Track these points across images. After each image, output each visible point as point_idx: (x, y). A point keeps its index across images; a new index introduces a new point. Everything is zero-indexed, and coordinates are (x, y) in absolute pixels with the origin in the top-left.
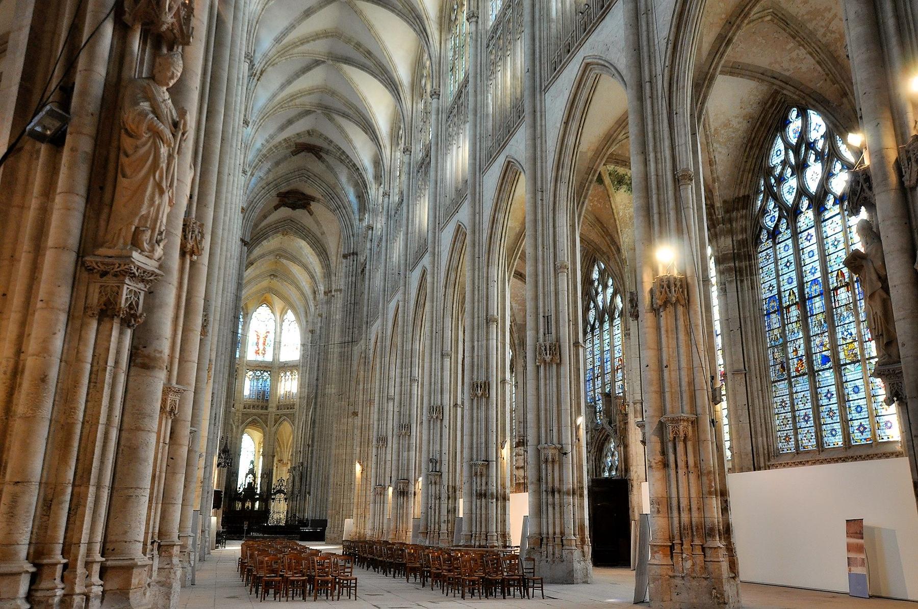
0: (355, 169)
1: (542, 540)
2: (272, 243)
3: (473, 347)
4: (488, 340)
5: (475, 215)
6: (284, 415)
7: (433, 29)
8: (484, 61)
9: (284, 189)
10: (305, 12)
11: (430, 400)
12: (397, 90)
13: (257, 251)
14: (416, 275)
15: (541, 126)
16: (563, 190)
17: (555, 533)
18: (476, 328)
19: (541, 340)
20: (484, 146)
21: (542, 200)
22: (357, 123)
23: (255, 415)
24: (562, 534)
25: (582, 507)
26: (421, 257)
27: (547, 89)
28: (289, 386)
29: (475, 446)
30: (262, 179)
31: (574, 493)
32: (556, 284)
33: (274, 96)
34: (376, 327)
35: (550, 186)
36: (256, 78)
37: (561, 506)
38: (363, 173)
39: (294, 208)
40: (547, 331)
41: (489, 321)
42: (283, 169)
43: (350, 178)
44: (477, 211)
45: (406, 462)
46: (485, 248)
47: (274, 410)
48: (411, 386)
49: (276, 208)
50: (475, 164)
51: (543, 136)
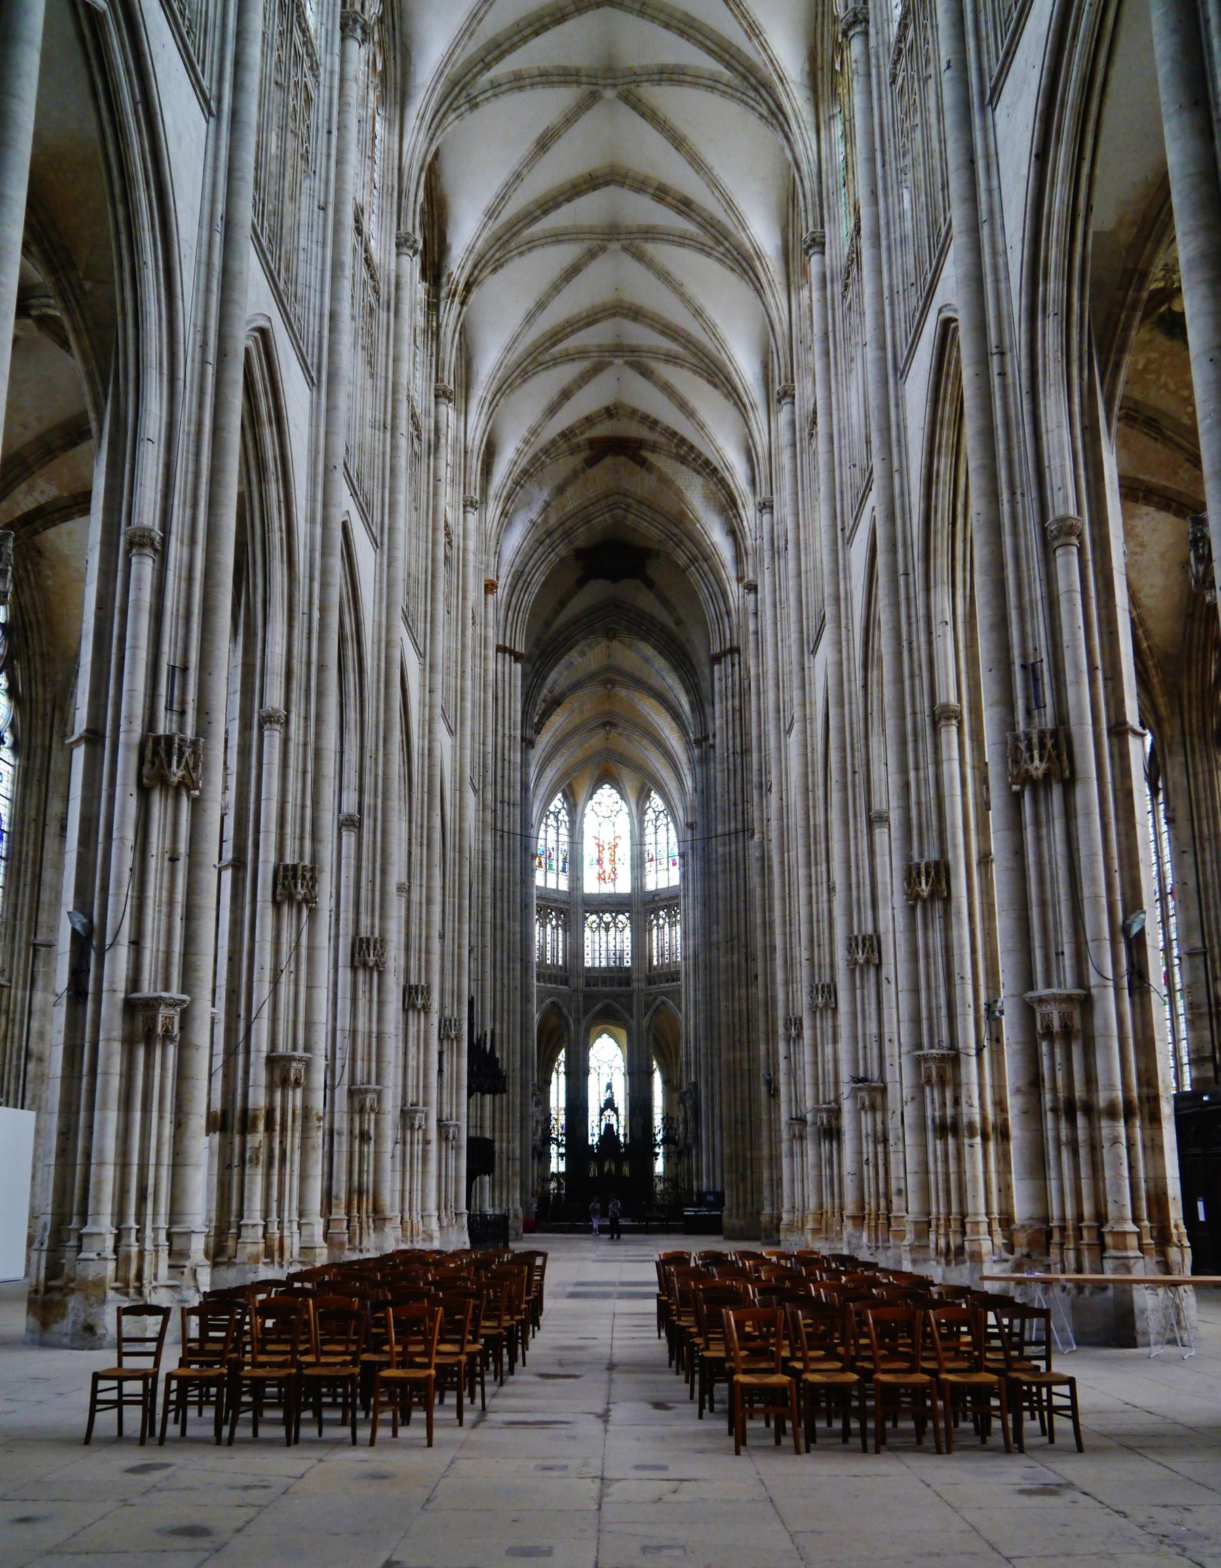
0: (710, 470)
1: (1049, 1234)
2: (585, 658)
3: (906, 785)
4: (938, 763)
5: (891, 478)
6: (662, 994)
7: (796, 99)
8: (887, 119)
9: (582, 537)
12: (753, 269)
13: (558, 677)
17: (1080, 1217)
18: (910, 738)
19: (1021, 727)
20: (900, 312)
21: (1002, 374)
22: (695, 370)
23: (607, 996)
24: (1101, 1217)
25: (1154, 1148)
28: (669, 939)
29: (924, 1014)
30: (533, 523)
31: (1129, 1114)
32: (1050, 579)
36: (457, 300)
37: (1094, 1147)
38: (727, 475)
39: (615, 578)
40: (1034, 703)
41: (940, 716)
42: (573, 500)
43: (710, 498)
44: (896, 465)
47: (643, 985)
49: (581, 583)
50: (885, 359)
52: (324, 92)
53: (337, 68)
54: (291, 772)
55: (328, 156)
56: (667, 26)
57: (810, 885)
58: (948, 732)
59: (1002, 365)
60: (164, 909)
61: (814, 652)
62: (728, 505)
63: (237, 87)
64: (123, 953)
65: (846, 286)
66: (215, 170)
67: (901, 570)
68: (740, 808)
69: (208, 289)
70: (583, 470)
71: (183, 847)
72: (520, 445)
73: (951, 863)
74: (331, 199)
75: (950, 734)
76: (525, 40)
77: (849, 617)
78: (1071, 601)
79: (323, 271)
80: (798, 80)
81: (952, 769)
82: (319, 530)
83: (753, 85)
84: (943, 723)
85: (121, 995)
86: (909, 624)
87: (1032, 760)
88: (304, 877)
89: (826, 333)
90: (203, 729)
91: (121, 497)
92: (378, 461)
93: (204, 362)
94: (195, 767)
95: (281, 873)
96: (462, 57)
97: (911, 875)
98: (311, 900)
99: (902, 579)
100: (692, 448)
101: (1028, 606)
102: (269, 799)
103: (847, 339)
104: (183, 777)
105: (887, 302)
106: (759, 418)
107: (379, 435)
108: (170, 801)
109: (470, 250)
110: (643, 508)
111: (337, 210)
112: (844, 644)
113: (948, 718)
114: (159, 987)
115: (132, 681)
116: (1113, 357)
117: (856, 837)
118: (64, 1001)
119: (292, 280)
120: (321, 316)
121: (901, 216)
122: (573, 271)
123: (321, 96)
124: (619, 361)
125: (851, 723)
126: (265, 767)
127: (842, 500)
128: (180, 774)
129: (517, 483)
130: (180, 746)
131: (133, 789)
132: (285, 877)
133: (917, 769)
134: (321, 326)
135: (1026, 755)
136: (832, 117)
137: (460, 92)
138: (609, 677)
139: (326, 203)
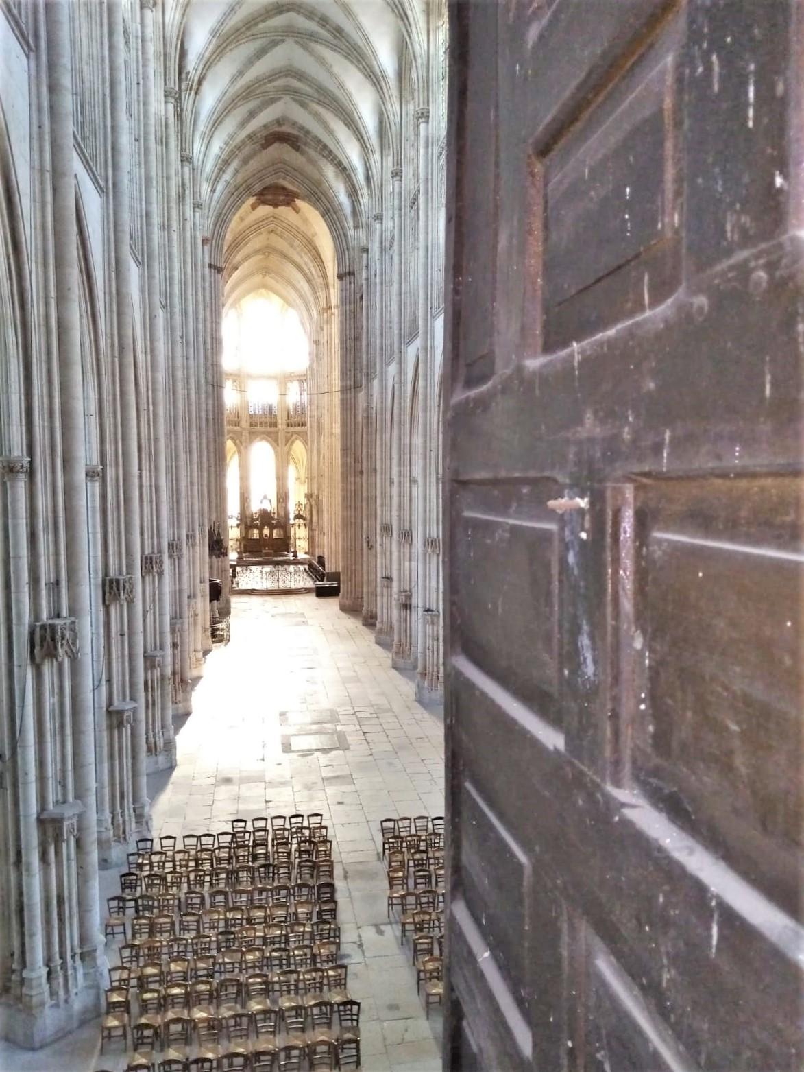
0: (343, 170)
36: (193, 92)
45: (407, 572)
47: (284, 426)
57: (400, 476)
70: (260, 151)
72: (222, 145)
74: (142, 133)
77: (432, 361)
79: (140, 184)
93: (113, 357)
109: (201, 57)
110: (297, 174)
111: (146, 140)
120: (141, 216)
124: (287, 98)
129: (221, 169)
134: (142, 224)
136: (437, 28)
138: (267, 250)
139: (139, 136)
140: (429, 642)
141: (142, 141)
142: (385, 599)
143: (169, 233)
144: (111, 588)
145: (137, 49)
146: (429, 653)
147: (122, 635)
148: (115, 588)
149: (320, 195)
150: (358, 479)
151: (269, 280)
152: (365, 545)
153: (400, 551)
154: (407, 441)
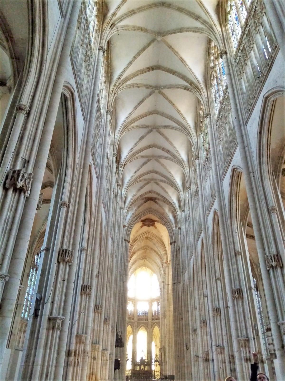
0: (170, 204)
4: (237, 265)
5: (221, 201)
6: (155, 323)
8: (216, 132)
10: (140, 138)
11: (212, 305)
12: (182, 164)
14: (199, 243)
15: (247, 141)
16: (265, 168)
18: (230, 259)
20: (221, 168)
22: (168, 184)
26: (201, 233)
27: (247, 122)
32: (271, 220)
33: (133, 176)
34: (186, 274)
35: (257, 168)
36: (122, 167)
38: (174, 205)
39: (149, 226)
41: (237, 254)
42: (141, 209)
43: (170, 209)
44: (222, 199)
45: (206, 342)
46: (228, 216)
47: (151, 320)
48: (204, 299)
50: (218, 178)
51: (249, 146)
52: (103, 124)
53: (105, 119)
54: (87, 262)
55: (103, 135)
56: (167, 118)
57: (199, 295)
58: (239, 258)
59: (253, 174)
60: (60, 293)
61: (197, 241)
62: (174, 212)
63: (90, 116)
64: (49, 305)
65: (204, 166)
66: (85, 131)
67: (225, 221)
68: (177, 277)
69: (82, 154)
70: (144, 204)
71: (66, 277)
73: (243, 289)
74: (103, 143)
75: (239, 258)
76: (139, 119)
77: (208, 233)
78: (277, 225)
79: (101, 156)
80: (193, 128)
81: (240, 266)
82: (97, 208)
83: (184, 129)
84: (238, 255)
85: (47, 316)
86: (228, 233)
87: (273, 262)
88: (89, 288)
89: (200, 175)
90: (73, 248)
91: (60, 195)
92: (107, 197)
93: (80, 168)
94: (71, 257)
95: (83, 287)
96: (127, 121)
97: (233, 292)
98: (90, 294)
99: (225, 223)
100: (167, 199)
101: (266, 226)
102: (82, 268)
103: (205, 176)
104: (69, 260)
105: (217, 166)
106: (182, 193)
107: (107, 191)
108: (64, 266)
110: (155, 212)
112: (207, 239)
113: (239, 254)
114: (57, 314)
115: (58, 236)
116: (278, 174)
117: (213, 283)
118: (32, 318)
119: (95, 157)
120: (100, 165)
121: (220, 150)
122: (145, 163)
123: (102, 124)
124: (152, 182)
125: (210, 256)
126: (81, 261)
127: (205, 208)
128: (68, 259)
130: (68, 252)
131: (56, 262)
132: (84, 288)
133: (232, 266)
135: (271, 261)
136: (200, 135)
137: (126, 128)
140: (220, 365)
141: (103, 145)
142: (196, 368)
143: (110, 192)
144: (62, 253)
145: (104, 123)
146: (221, 371)
147: (64, 281)
148: (64, 253)
149: (163, 217)
150: (181, 322)
151: (146, 262)
152: (185, 348)
153: (201, 332)
154: (201, 279)
